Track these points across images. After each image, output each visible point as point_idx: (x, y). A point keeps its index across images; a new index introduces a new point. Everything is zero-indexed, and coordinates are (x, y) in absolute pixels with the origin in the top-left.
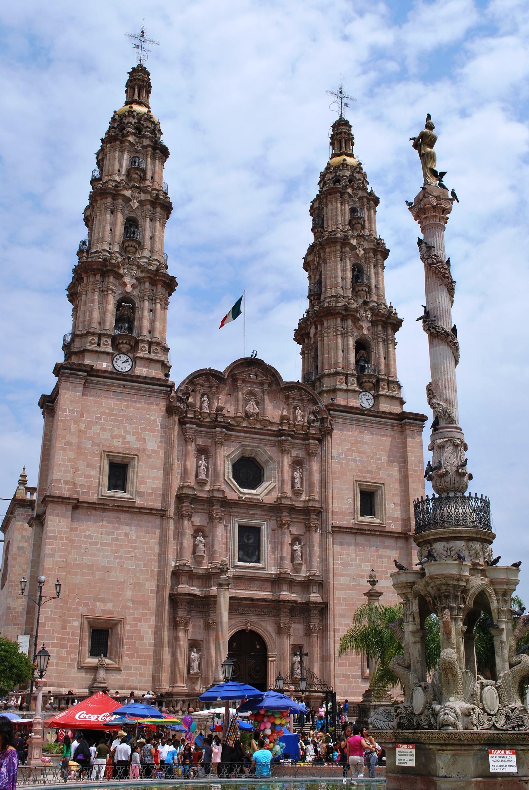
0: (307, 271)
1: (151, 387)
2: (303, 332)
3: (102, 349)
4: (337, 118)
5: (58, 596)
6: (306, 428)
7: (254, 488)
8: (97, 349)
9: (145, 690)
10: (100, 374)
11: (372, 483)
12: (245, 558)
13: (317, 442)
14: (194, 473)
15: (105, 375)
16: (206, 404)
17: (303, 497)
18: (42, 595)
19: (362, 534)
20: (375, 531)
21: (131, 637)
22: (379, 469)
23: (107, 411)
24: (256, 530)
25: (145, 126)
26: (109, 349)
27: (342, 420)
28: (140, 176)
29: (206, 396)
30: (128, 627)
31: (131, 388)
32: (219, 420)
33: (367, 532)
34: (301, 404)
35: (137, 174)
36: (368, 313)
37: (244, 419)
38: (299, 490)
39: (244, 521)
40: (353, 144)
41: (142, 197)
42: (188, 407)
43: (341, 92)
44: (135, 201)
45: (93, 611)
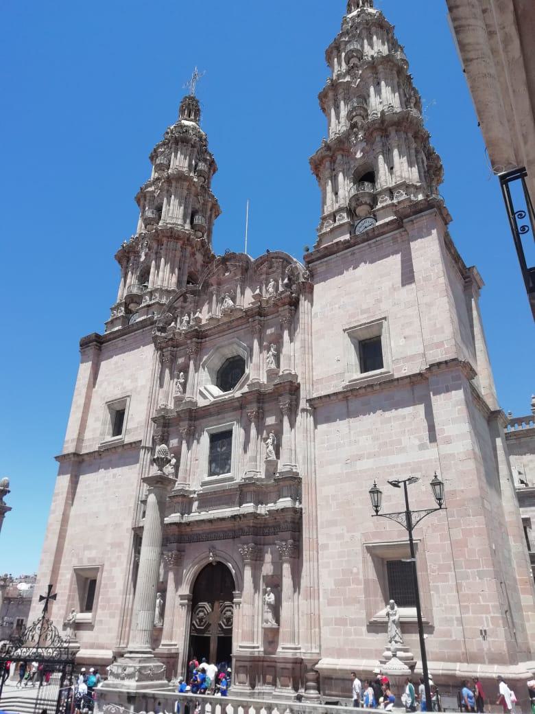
9: (107, 649)
11: (368, 323)
12: (218, 470)
21: (106, 585)
22: (379, 301)
30: (105, 574)
45: (80, 560)
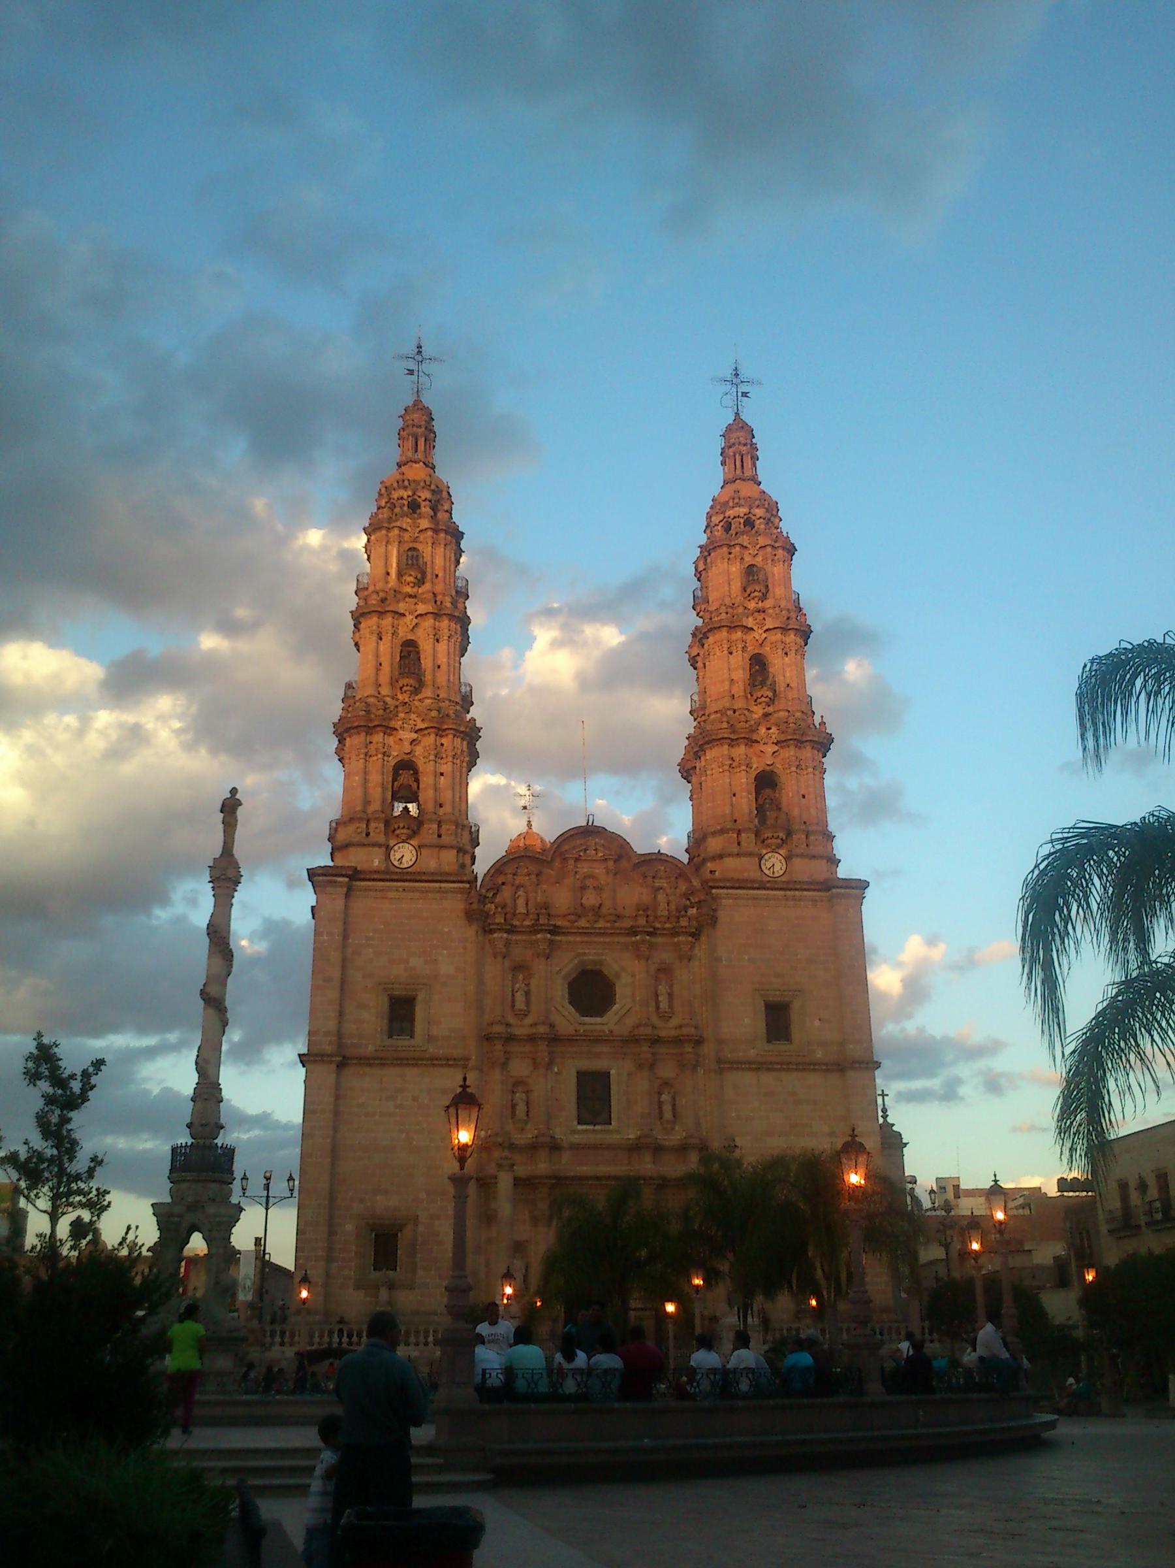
0: (695, 669)
1: (443, 885)
2: (688, 767)
3: (372, 839)
4: (730, 419)
5: (292, 1194)
6: (673, 919)
7: (601, 1016)
8: (366, 841)
10: (368, 877)
13: (690, 939)
14: (510, 1004)
15: (375, 876)
16: (521, 902)
17: (674, 1022)
18: (270, 1195)
19: (769, 1069)
20: (789, 1063)
23: (382, 927)
24: (603, 1078)
25: (423, 498)
26: (381, 839)
27: (731, 901)
28: (416, 578)
29: (522, 889)
31: (413, 890)
32: (541, 922)
33: (775, 1066)
34: (667, 883)
35: (411, 575)
36: (771, 731)
37: (579, 917)
38: (666, 1012)
39: (586, 1064)
40: (755, 458)
41: (421, 608)
42: (496, 907)
43: (737, 375)
44: (411, 617)
